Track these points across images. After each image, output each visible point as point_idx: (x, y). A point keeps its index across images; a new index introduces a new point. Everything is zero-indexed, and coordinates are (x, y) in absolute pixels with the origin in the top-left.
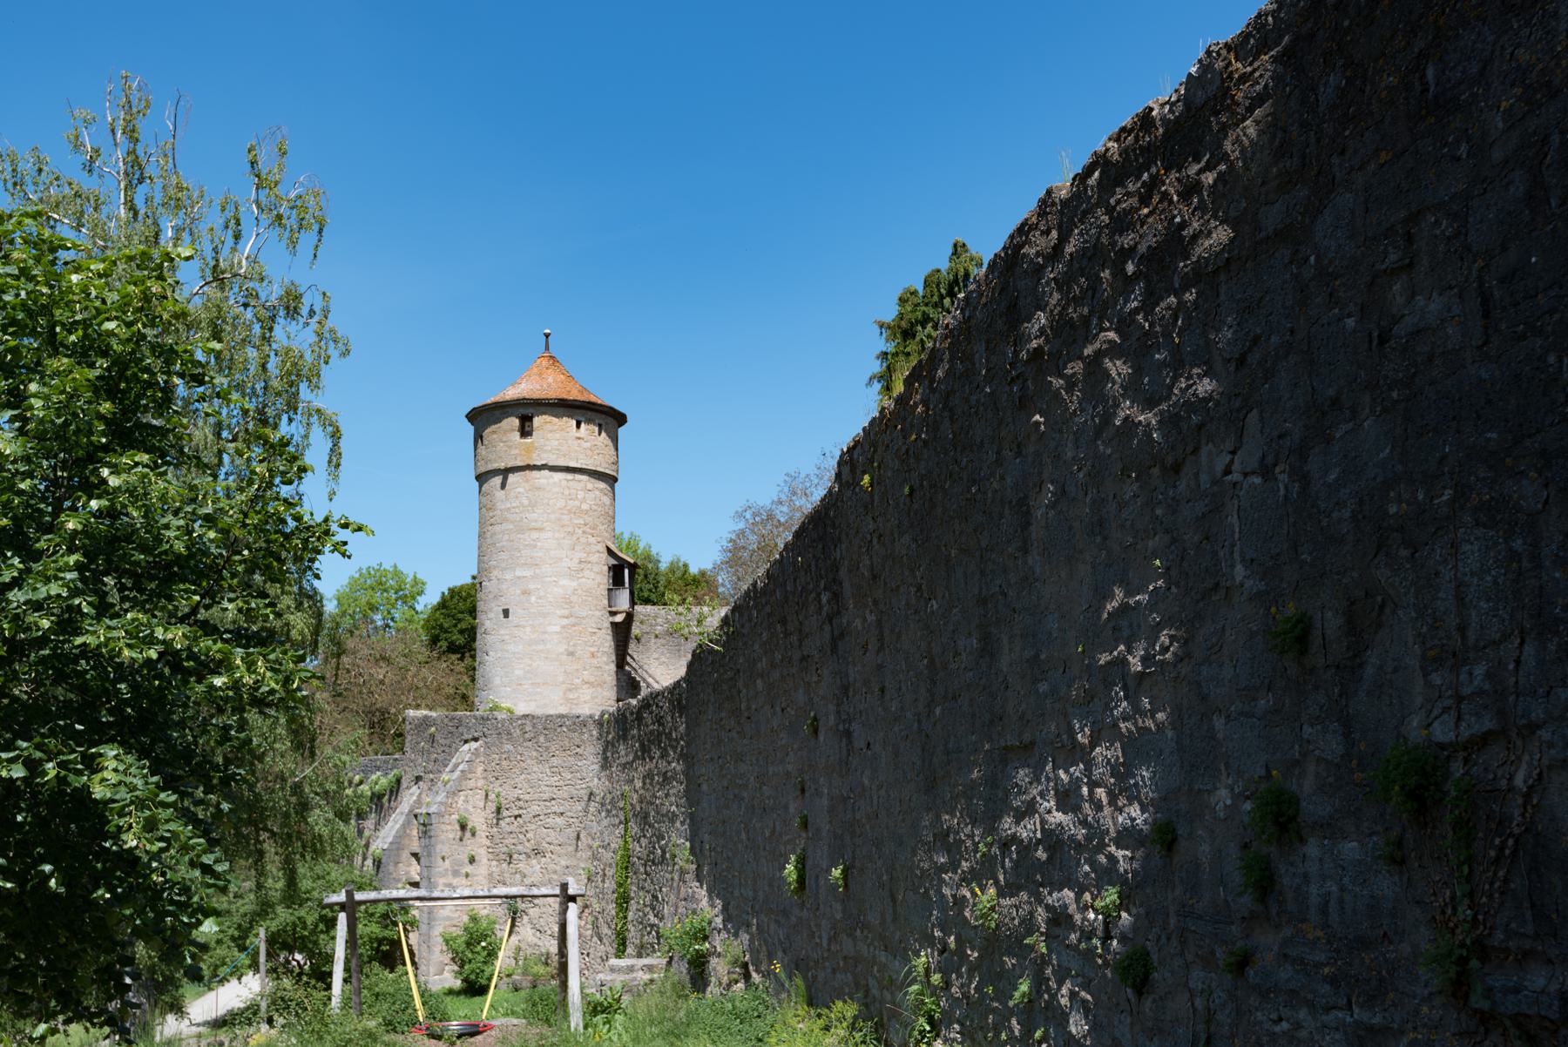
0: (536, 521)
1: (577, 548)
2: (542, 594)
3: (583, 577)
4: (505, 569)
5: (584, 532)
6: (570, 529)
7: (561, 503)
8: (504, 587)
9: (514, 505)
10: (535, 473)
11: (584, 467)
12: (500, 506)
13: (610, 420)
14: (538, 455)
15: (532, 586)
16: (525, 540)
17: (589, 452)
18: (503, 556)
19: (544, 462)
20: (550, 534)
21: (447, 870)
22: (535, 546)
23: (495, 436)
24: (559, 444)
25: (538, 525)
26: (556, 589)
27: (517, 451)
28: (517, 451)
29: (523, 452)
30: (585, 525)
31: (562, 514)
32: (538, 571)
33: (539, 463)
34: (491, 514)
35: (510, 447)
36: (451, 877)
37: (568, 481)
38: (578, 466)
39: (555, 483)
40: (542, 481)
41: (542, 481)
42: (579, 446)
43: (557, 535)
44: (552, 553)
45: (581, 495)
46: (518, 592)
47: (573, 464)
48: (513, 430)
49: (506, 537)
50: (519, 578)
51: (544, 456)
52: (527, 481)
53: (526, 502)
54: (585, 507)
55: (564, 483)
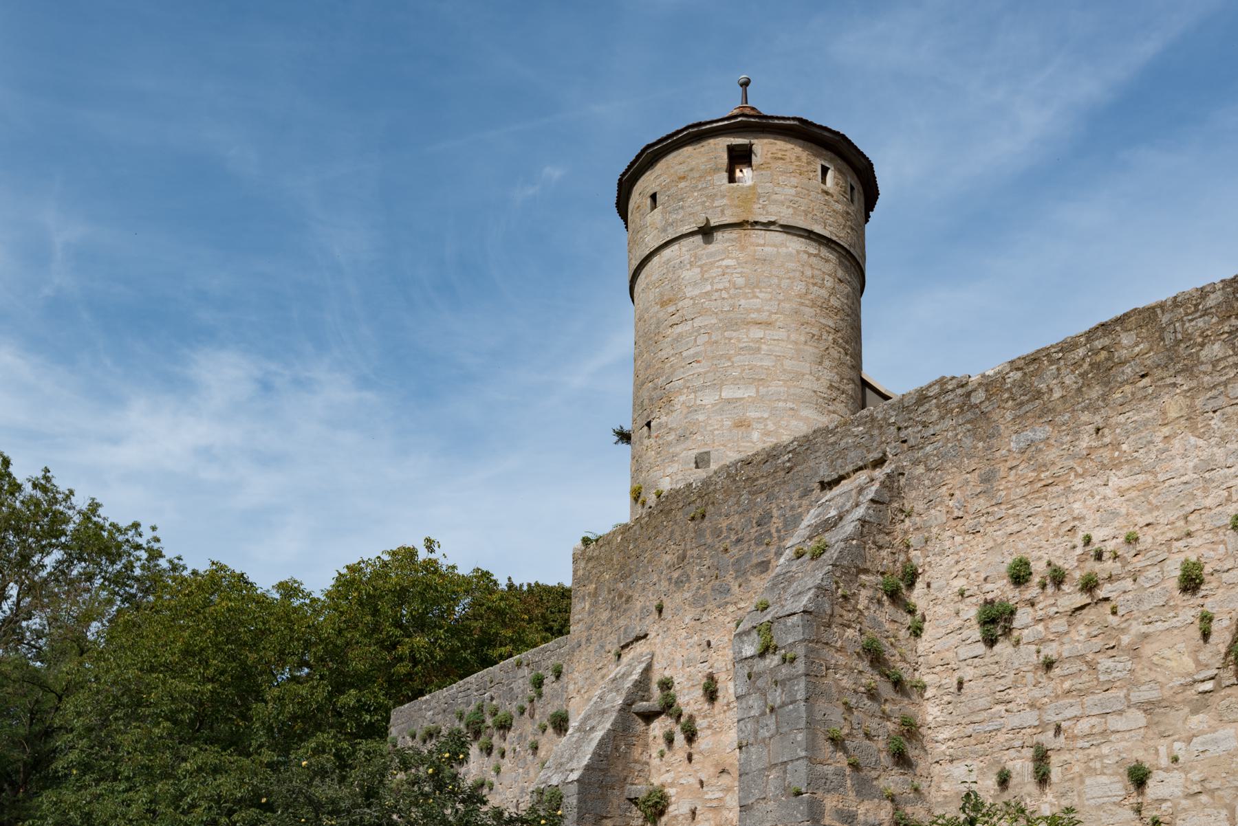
0: (759, 311)
1: (827, 363)
2: (771, 427)
3: (834, 412)
4: (704, 387)
5: (835, 341)
6: (815, 331)
7: (799, 287)
8: (701, 418)
9: (720, 286)
10: (758, 236)
11: (834, 238)
12: (691, 292)
13: (861, 188)
14: (764, 207)
15: (752, 414)
16: (739, 340)
17: (841, 220)
18: (698, 368)
19: (772, 220)
20: (782, 334)
21: (839, 773)
22: (759, 349)
23: (682, 184)
24: (797, 194)
25: (764, 316)
26: (794, 423)
27: (725, 201)
28: (725, 201)
29: (736, 202)
30: (837, 331)
31: (802, 304)
32: (762, 390)
33: (765, 220)
34: (671, 309)
35: (712, 197)
36: (852, 795)
37: (810, 255)
38: (826, 233)
39: (790, 255)
40: (768, 249)
41: (768, 249)
42: (827, 203)
43: (793, 337)
44: (788, 364)
45: (829, 283)
46: (728, 423)
47: (818, 229)
48: (716, 170)
49: (703, 339)
50: (729, 401)
51: (773, 208)
52: (743, 248)
53: (740, 281)
54: (834, 302)
55: (805, 256)
